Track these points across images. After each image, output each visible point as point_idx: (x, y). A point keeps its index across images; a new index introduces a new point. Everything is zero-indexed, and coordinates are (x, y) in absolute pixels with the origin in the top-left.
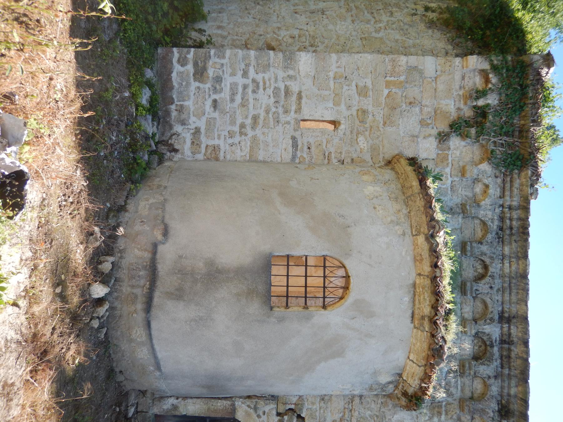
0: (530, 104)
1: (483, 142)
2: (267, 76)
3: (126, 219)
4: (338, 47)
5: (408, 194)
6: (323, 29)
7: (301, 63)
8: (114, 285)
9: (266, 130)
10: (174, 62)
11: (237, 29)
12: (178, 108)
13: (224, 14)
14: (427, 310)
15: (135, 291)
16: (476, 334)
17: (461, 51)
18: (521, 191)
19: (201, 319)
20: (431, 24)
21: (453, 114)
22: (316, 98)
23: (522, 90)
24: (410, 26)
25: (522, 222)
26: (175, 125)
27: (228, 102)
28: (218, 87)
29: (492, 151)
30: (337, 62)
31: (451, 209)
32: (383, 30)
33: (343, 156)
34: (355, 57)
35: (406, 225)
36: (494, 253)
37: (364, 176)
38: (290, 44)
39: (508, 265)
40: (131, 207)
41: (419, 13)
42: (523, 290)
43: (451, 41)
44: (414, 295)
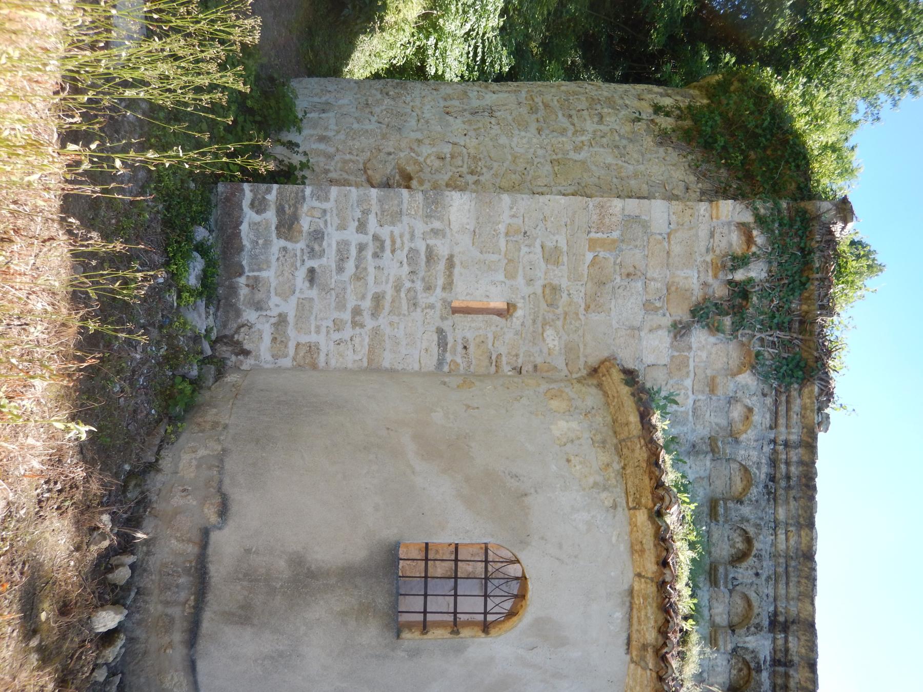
0: (817, 279)
1: (744, 339)
2: (397, 230)
3: (159, 485)
4: (513, 176)
5: (622, 436)
6: (491, 143)
7: (453, 210)
8: (135, 600)
9: (395, 319)
11: (350, 143)
12: (251, 282)
14: (651, 636)
15: (169, 611)
16: (734, 650)
17: (709, 185)
18: (803, 417)
19: (281, 655)
20: (663, 138)
21: (695, 293)
22: (477, 266)
23: (804, 256)
24: (631, 140)
25: (805, 468)
26: (245, 311)
27: (334, 273)
28: (317, 247)
29: (758, 354)
30: (511, 208)
31: (694, 446)
32: (586, 148)
33: (520, 361)
34: (541, 200)
35: (618, 490)
36: (761, 519)
37: (552, 402)
38: (436, 170)
39: (783, 537)
40: (166, 463)
41: (644, 117)
42: (806, 578)
43: (694, 168)
44: (631, 609)
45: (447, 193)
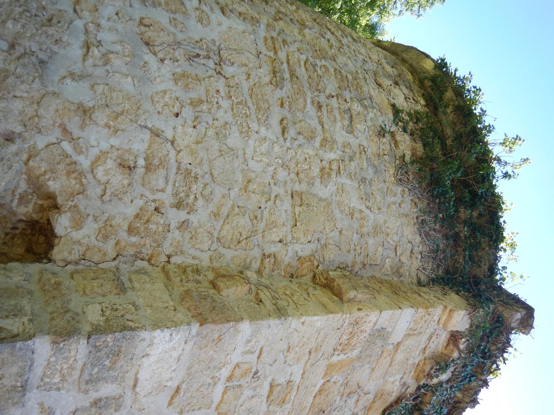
6: (216, 145)
30: (249, 341)
45: (145, 334)
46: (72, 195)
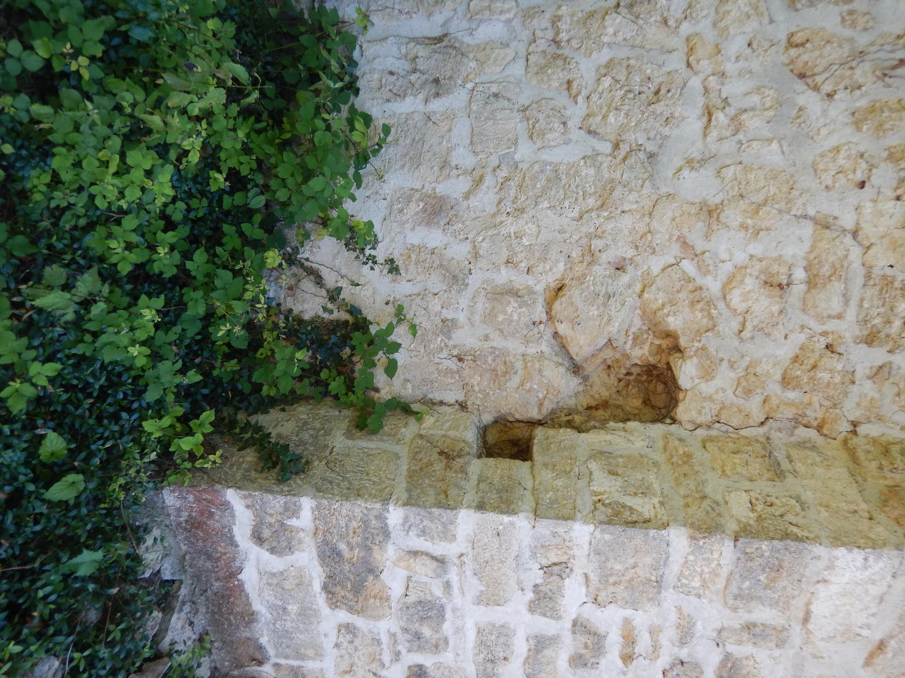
2: (641, 619)
10: (238, 538)
13: (456, 99)
28: (427, 632)
38: (758, 329)
45: (819, 550)
46: (699, 333)
